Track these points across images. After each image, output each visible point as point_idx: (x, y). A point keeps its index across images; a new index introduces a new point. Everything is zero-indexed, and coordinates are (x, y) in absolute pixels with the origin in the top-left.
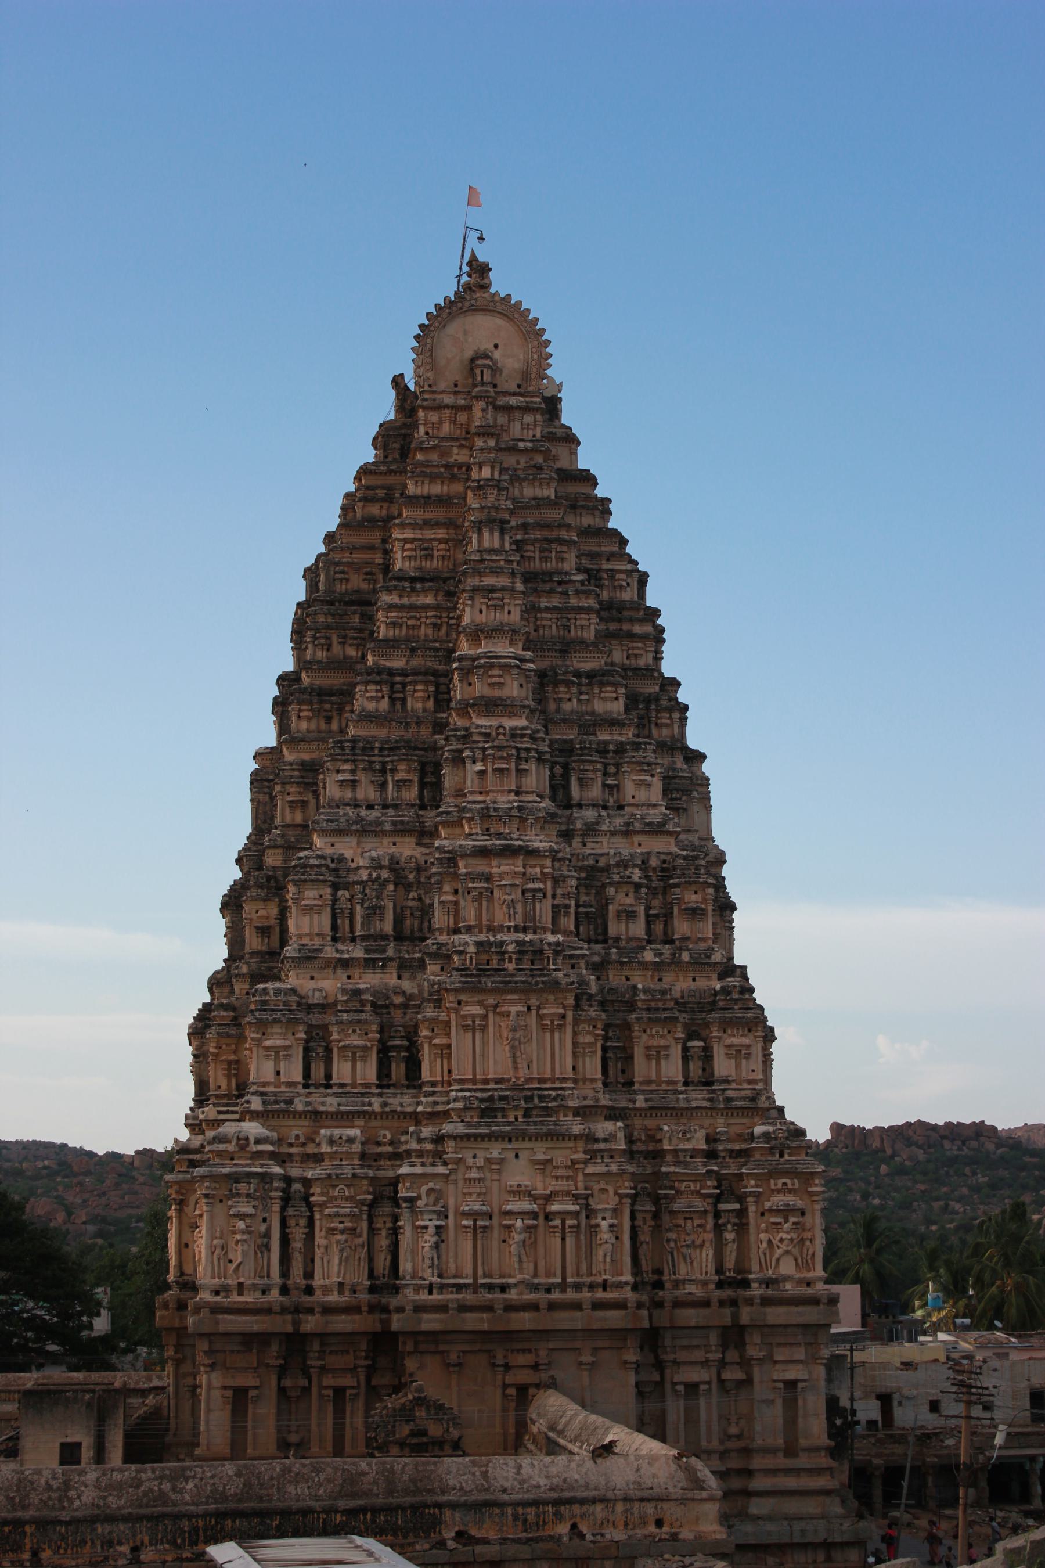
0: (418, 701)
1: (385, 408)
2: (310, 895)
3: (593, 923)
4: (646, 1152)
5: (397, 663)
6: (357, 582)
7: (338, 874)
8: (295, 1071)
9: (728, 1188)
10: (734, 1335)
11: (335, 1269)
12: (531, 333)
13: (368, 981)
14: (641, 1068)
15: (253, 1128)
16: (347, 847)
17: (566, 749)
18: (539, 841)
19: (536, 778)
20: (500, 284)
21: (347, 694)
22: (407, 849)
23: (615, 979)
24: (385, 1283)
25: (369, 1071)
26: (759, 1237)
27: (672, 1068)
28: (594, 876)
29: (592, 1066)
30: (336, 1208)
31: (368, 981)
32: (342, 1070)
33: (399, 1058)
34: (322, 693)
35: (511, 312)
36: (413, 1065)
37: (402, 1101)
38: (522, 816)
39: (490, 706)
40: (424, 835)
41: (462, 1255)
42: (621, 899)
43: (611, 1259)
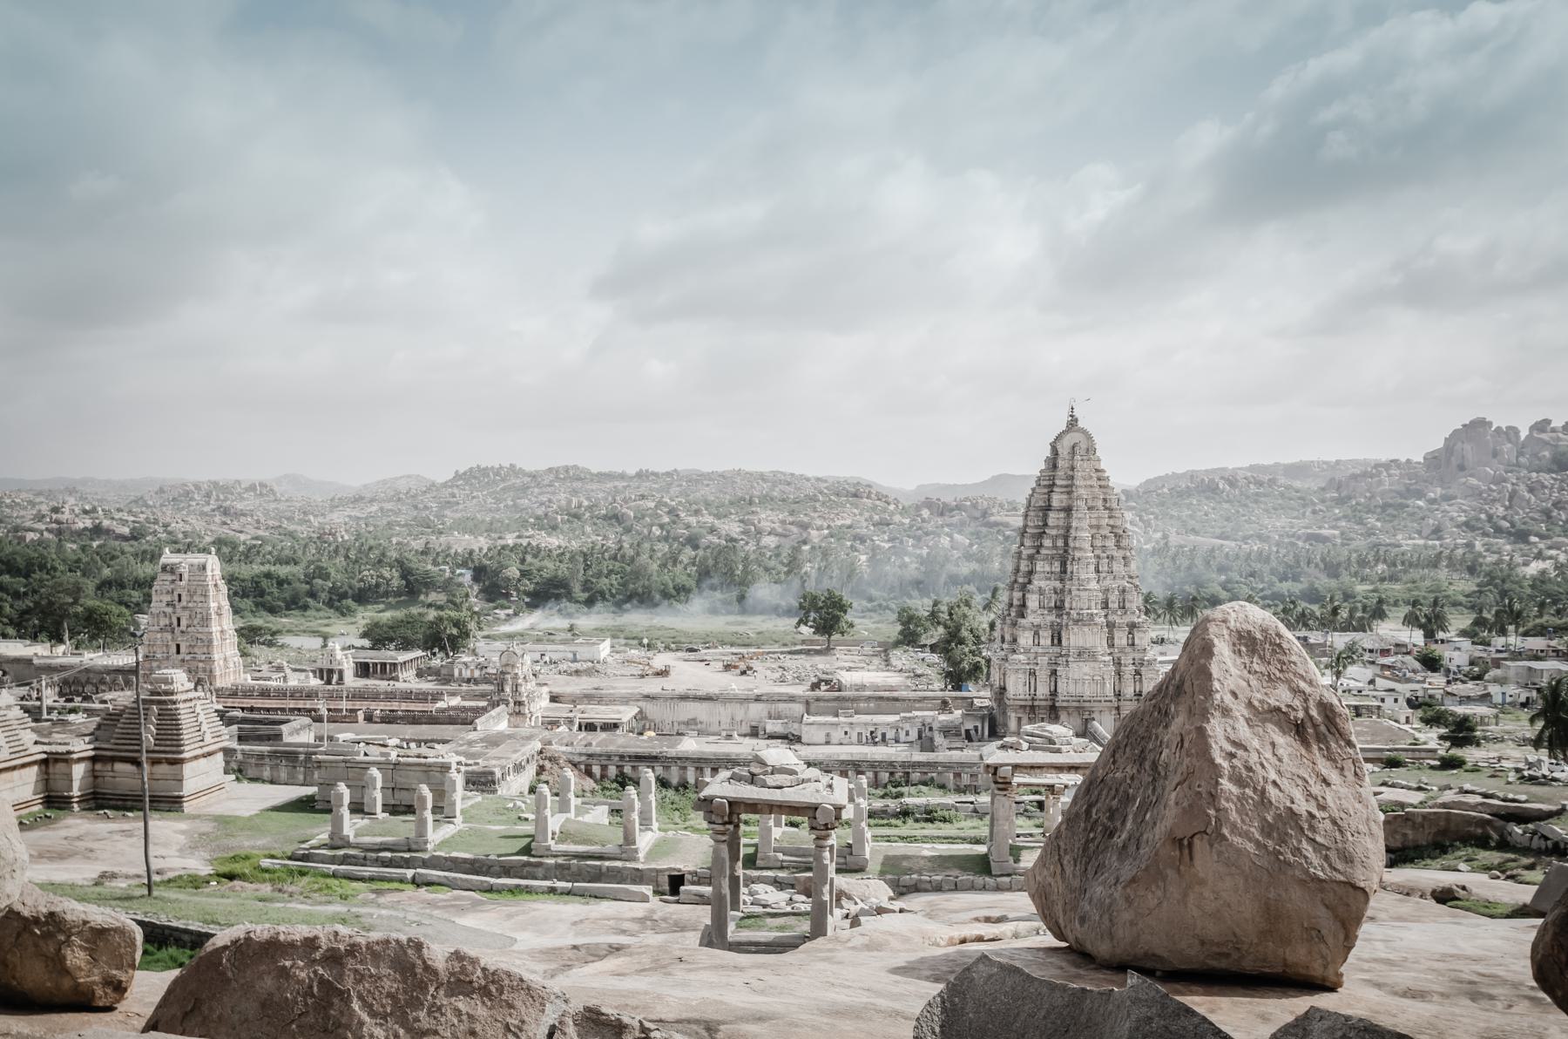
0: (1060, 543)
1: (1048, 453)
3: (1105, 605)
5: (1054, 532)
6: (1041, 503)
7: (1041, 591)
9: (1138, 673)
11: (1043, 690)
14: (1116, 641)
15: (1021, 657)
17: (1098, 557)
20: (1081, 424)
22: (1058, 584)
23: (1110, 618)
24: (1054, 693)
27: (1124, 642)
30: (1043, 675)
32: (1042, 642)
33: (1057, 639)
35: (1084, 432)
37: (1057, 649)
40: (1062, 580)
41: (1071, 688)
43: (1109, 690)
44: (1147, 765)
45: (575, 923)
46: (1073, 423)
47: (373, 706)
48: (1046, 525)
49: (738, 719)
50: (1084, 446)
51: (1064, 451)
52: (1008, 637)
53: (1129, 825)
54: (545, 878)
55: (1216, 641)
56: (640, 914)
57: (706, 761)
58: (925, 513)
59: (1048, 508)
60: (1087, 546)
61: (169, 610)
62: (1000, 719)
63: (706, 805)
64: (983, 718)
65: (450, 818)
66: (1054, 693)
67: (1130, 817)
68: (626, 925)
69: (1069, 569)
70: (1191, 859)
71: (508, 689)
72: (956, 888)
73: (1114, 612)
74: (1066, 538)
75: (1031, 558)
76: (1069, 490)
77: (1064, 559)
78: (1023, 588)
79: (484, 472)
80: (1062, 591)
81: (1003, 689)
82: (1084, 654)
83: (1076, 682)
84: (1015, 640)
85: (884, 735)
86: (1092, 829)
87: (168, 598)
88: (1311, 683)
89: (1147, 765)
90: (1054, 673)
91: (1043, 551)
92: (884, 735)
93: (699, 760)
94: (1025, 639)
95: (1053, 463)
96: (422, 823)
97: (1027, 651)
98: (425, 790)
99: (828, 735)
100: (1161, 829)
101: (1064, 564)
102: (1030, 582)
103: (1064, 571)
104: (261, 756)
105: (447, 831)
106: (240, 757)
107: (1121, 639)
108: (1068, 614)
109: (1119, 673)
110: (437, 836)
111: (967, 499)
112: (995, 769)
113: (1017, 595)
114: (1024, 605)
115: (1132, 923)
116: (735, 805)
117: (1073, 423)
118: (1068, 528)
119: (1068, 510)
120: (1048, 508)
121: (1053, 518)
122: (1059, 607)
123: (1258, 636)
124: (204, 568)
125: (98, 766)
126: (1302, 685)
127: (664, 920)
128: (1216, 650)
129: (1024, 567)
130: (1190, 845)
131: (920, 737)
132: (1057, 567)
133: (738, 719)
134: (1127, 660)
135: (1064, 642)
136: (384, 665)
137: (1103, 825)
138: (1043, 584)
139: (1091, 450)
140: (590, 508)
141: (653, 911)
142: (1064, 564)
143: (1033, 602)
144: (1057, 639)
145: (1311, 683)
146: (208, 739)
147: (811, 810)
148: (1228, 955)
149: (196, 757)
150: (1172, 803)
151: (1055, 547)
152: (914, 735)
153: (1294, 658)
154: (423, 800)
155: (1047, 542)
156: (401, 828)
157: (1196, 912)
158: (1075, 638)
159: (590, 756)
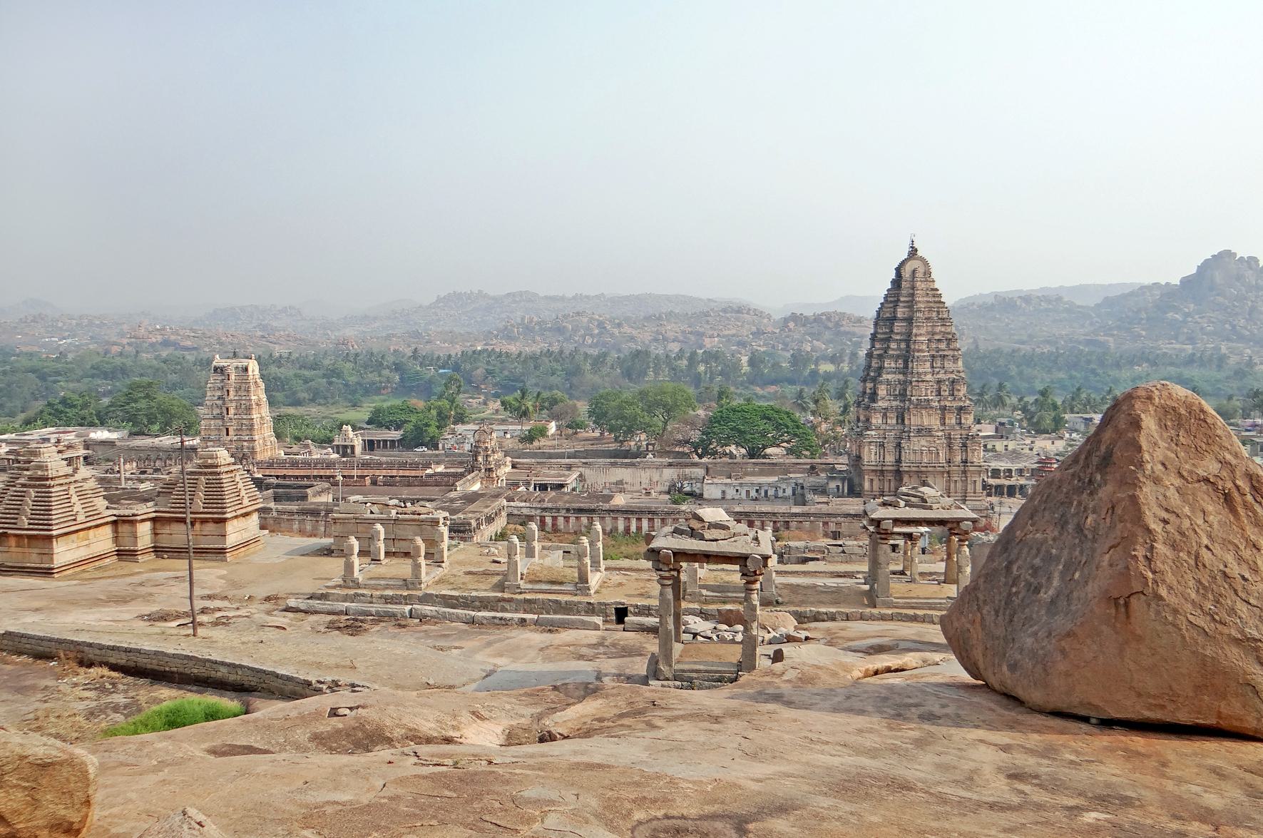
0: (903, 345)
2: (883, 387)
4: (949, 438)
7: (888, 383)
8: (880, 421)
9: (965, 445)
10: (964, 472)
12: (926, 263)
13: (894, 403)
16: (890, 377)
17: (933, 356)
19: (928, 364)
20: (919, 253)
21: (888, 340)
22: (901, 377)
24: (899, 461)
25: (894, 421)
26: (970, 454)
27: (953, 421)
28: (939, 382)
30: (890, 446)
31: (894, 403)
33: (901, 418)
34: (882, 340)
35: (922, 259)
36: (903, 420)
37: (900, 427)
38: (926, 374)
40: (904, 374)
42: (944, 387)
44: (1071, 527)
45: (541, 650)
46: (913, 252)
47: (377, 473)
48: (892, 331)
49: (654, 480)
50: (921, 270)
51: (906, 274)
52: (862, 418)
53: (1056, 582)
54: (516, 611)
55: (1143, 416)
56: (594, 641)
57: (632, 512)
58: (791, 325)
59: (894, 318)
60: (924, 347)
61: (220, 402)
62: (856, 480)
63: (654, 554)
64: (843, 480)
65: (439, 563)
66: (899, 461)
67: (1056, 575)
68: (584, 651)
70: (1128, 617)
71: (480, 459)
72: (848, 618)
73: (946, 399)
74: (908, 341)
75: (880, 356)
76: (911, 304)
77: (907, 358)
78: (874, 380)
79: (458, 296)
80: (905, 382)
81: (859, 458)
82: (924, 432)
83: (915, 452)
84: (868, 420)
85: (766, 492)
86: (1014, 584)
87: (219, 393)
88: (1236, 455)
89: (1071, 527)
90: (899, 445)
91: (891, 352)
92: (766, 492)
93: (626, 512)
94: (877, 420)
95: (897, 283)
96: (417, 567)
97: (878, 429)
98: (419, 541)
99: (724, 492)
100: (1093, 588)
101: (906, 362)
102: (880, 375)
103: (906, 367)
104: (291, 513)
105: (438, 573)
106: (275, 514)
107: (951, 420)
109: (950, 446)
110: (429, 577)
111: (823, 314)
112: (877, 523)
113: (870, 385)
115: (1068, 674)
116: (680, 555)
117: (913, 252)
118: (909, 334)
119: (909, 320)
120: (894, 318)
121: (899, 327)
122: (903, 396)
123: (1183, 411)
124: (246, 369)
125: (158, 525)
126: (1228, 457)
127: (614, 645)
128: (1144, 425)
129: (875, 364)
130: (1127, 605)
131: (794, 494)
132: (900, 363)
133: (654, 480)
134: (956, 434)
135: (906, 422)
136: (385, 441)
137: (1026, 580)
138: (890, 377)
139: (928, 273)
140: (538, 323)
141: (604, 638)
142: (906, 362)
143: (882, 391)
144: (901, 418)
145: (1236, 455)
146: (246, 502)
147: (741, 559)
148: (1163, 707)
149: (236, 517)
150: (1105, 564)
151: (899, 349)
152: (789, 492)
153: (1219, 432)
154: (418, 548)
155: (893, 345)
156: (402, 568)
157: (1132, 666)
158: (914, 420)
159: (544, 509)
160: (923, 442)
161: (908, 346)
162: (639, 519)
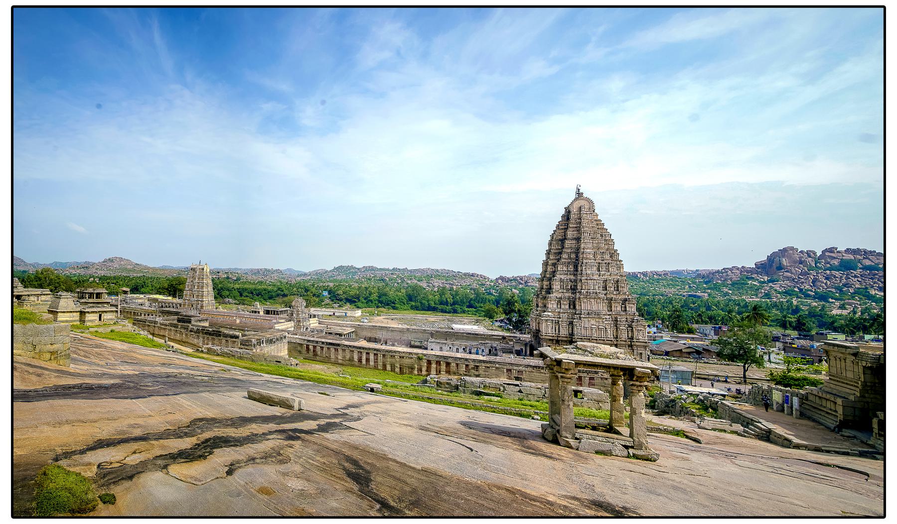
0: (573, 256)
7: (561, 280)
11: (564, 332)
13: (567, 295)
18: (596, 277)
19: (595, 268)
22: (572, 277)
25: (567, 307)
29: (605, 309)
31: (567, 295)
33: (573, 304)
39: (587, 259)
64: (526, 345)
69: (579, 269)
75: (554, 265)
78: (550, 279)
80: (576, 281)
83: (585, 328)
90: (571, 323)
101: (576, 267)
108: (580, 292)
113: (545, 283)
114: (550, 288)
118: (578, 249)
122: (574, 289)
129: (549, 269)
132: (571, 268)
135: (577, 307)
138: (562, 277)
142: (576, 267)
143: (556, 286)
144: (573, 304)
158: (584, 306)
160: (593, 322)
161: (577, 256)
162: (368, 354)
